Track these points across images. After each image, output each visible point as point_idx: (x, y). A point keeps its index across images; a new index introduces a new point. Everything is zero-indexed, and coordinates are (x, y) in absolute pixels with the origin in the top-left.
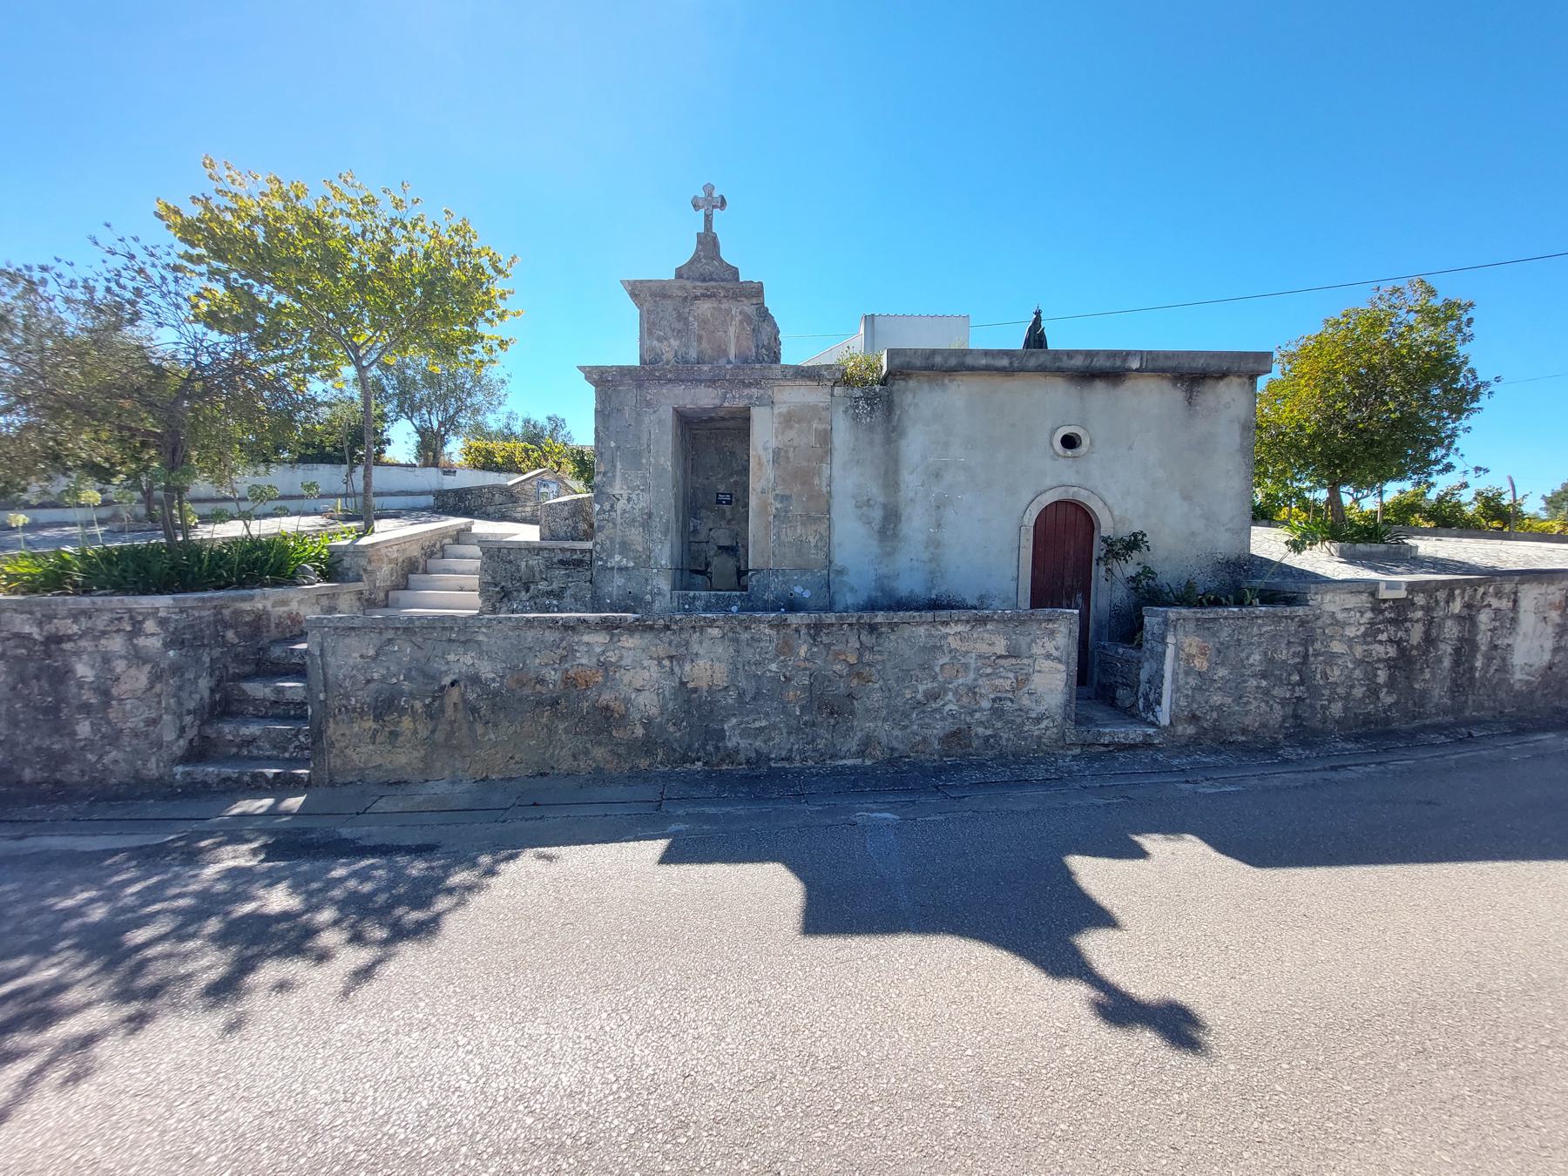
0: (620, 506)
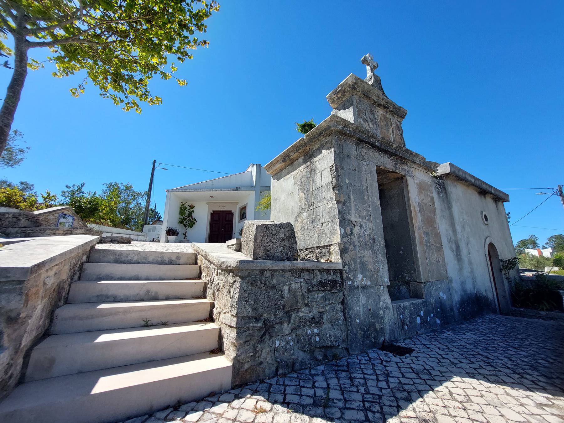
0: (356, 230)
